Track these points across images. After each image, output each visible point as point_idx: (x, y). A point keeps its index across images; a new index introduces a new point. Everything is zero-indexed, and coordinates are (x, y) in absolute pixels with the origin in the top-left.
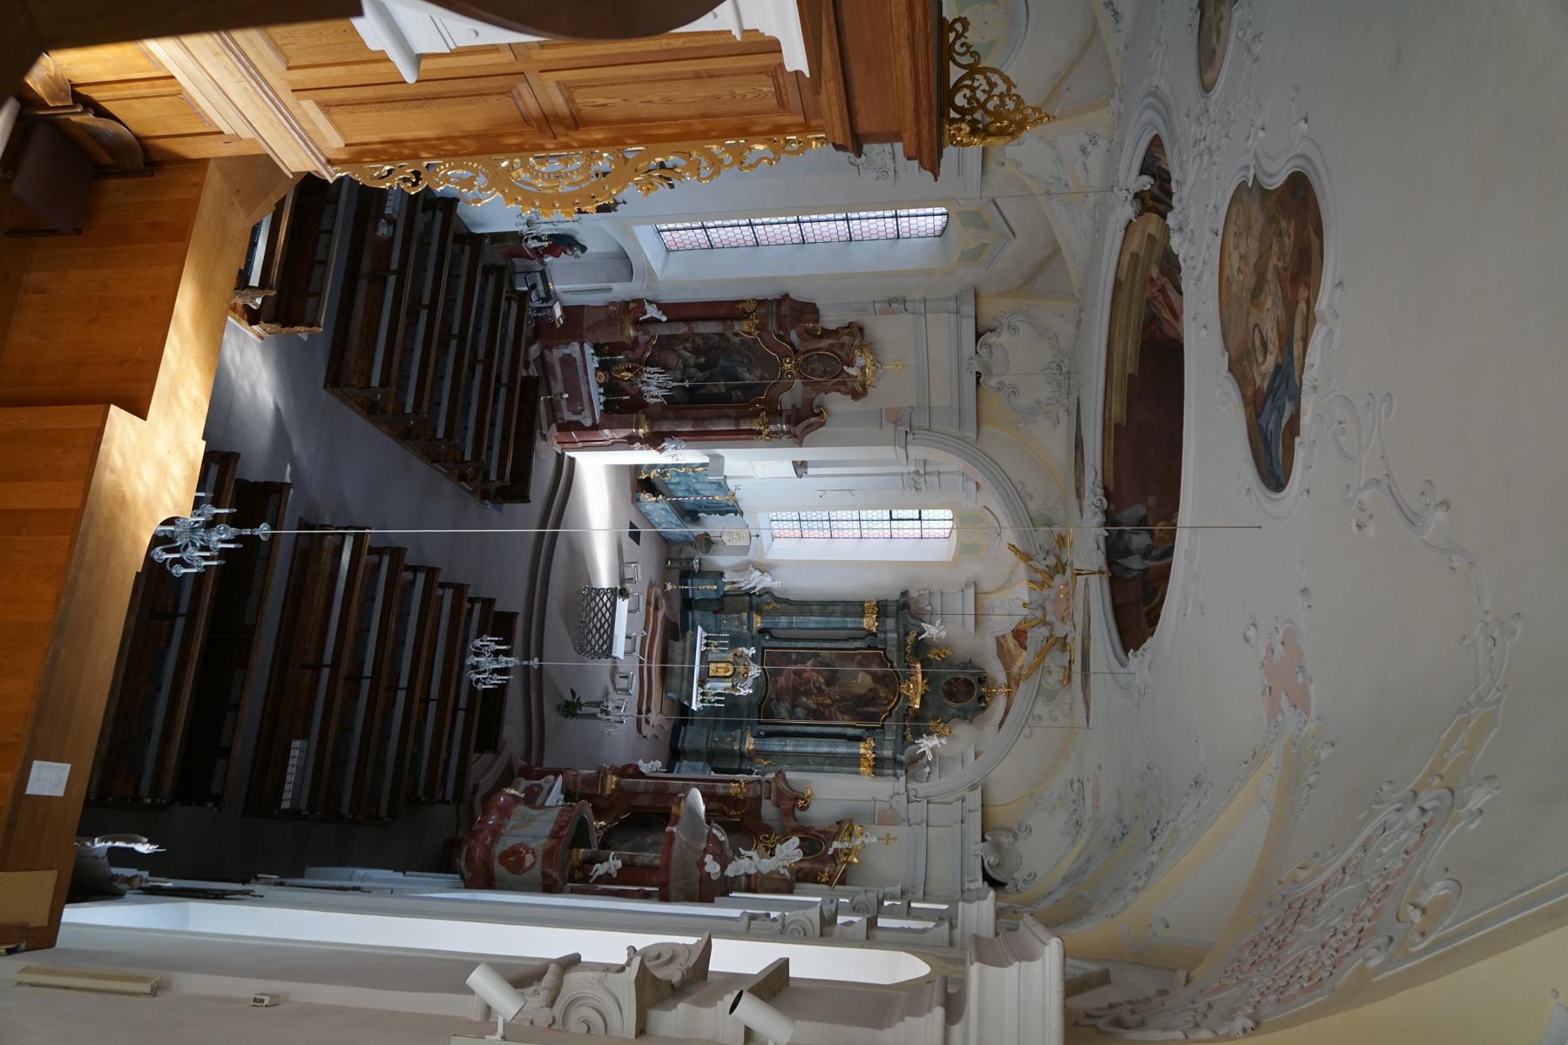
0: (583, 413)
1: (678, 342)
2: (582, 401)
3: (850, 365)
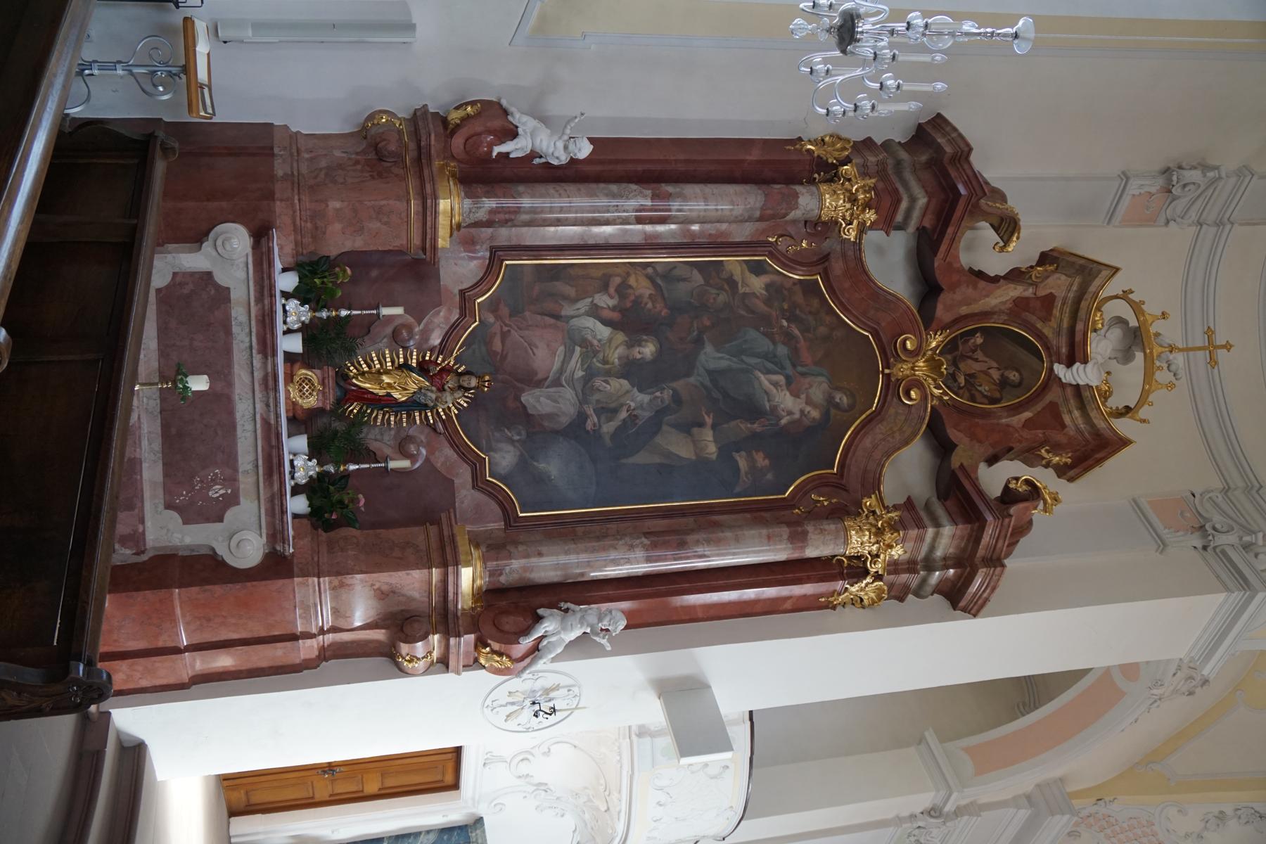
0: (229, 515)
1: (570, 291)
2: (231, 460)
3: (1076, 354)
